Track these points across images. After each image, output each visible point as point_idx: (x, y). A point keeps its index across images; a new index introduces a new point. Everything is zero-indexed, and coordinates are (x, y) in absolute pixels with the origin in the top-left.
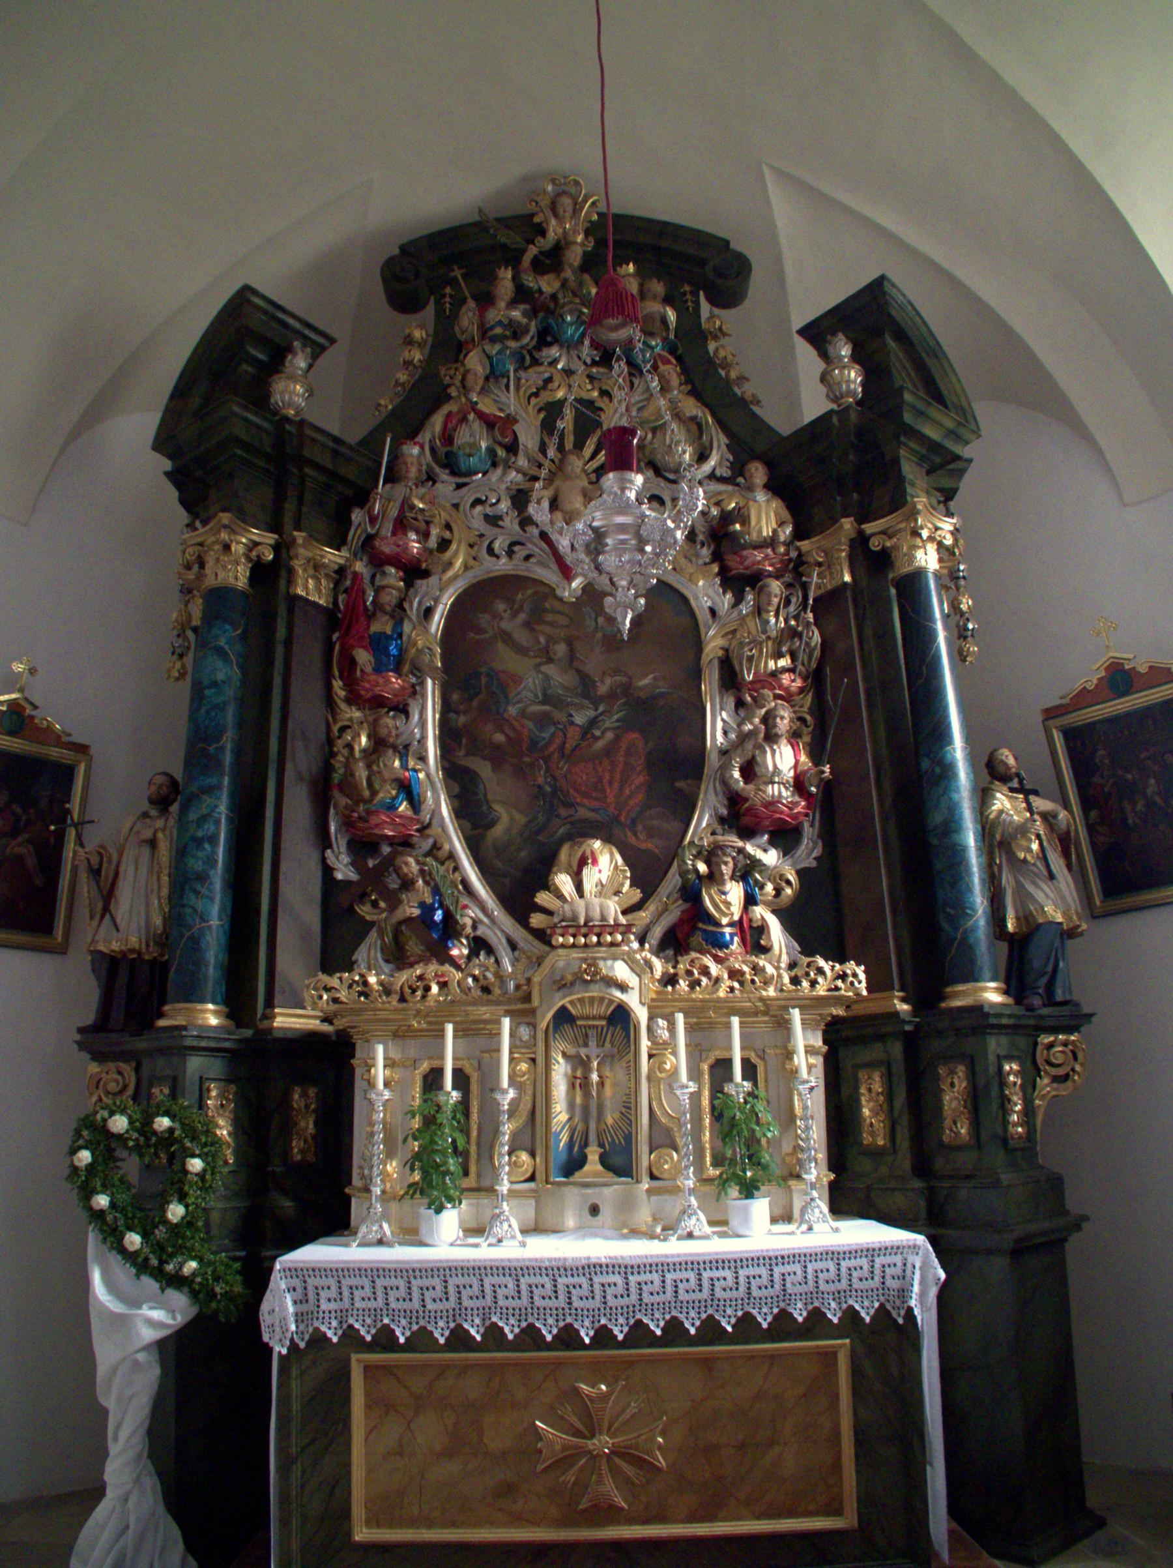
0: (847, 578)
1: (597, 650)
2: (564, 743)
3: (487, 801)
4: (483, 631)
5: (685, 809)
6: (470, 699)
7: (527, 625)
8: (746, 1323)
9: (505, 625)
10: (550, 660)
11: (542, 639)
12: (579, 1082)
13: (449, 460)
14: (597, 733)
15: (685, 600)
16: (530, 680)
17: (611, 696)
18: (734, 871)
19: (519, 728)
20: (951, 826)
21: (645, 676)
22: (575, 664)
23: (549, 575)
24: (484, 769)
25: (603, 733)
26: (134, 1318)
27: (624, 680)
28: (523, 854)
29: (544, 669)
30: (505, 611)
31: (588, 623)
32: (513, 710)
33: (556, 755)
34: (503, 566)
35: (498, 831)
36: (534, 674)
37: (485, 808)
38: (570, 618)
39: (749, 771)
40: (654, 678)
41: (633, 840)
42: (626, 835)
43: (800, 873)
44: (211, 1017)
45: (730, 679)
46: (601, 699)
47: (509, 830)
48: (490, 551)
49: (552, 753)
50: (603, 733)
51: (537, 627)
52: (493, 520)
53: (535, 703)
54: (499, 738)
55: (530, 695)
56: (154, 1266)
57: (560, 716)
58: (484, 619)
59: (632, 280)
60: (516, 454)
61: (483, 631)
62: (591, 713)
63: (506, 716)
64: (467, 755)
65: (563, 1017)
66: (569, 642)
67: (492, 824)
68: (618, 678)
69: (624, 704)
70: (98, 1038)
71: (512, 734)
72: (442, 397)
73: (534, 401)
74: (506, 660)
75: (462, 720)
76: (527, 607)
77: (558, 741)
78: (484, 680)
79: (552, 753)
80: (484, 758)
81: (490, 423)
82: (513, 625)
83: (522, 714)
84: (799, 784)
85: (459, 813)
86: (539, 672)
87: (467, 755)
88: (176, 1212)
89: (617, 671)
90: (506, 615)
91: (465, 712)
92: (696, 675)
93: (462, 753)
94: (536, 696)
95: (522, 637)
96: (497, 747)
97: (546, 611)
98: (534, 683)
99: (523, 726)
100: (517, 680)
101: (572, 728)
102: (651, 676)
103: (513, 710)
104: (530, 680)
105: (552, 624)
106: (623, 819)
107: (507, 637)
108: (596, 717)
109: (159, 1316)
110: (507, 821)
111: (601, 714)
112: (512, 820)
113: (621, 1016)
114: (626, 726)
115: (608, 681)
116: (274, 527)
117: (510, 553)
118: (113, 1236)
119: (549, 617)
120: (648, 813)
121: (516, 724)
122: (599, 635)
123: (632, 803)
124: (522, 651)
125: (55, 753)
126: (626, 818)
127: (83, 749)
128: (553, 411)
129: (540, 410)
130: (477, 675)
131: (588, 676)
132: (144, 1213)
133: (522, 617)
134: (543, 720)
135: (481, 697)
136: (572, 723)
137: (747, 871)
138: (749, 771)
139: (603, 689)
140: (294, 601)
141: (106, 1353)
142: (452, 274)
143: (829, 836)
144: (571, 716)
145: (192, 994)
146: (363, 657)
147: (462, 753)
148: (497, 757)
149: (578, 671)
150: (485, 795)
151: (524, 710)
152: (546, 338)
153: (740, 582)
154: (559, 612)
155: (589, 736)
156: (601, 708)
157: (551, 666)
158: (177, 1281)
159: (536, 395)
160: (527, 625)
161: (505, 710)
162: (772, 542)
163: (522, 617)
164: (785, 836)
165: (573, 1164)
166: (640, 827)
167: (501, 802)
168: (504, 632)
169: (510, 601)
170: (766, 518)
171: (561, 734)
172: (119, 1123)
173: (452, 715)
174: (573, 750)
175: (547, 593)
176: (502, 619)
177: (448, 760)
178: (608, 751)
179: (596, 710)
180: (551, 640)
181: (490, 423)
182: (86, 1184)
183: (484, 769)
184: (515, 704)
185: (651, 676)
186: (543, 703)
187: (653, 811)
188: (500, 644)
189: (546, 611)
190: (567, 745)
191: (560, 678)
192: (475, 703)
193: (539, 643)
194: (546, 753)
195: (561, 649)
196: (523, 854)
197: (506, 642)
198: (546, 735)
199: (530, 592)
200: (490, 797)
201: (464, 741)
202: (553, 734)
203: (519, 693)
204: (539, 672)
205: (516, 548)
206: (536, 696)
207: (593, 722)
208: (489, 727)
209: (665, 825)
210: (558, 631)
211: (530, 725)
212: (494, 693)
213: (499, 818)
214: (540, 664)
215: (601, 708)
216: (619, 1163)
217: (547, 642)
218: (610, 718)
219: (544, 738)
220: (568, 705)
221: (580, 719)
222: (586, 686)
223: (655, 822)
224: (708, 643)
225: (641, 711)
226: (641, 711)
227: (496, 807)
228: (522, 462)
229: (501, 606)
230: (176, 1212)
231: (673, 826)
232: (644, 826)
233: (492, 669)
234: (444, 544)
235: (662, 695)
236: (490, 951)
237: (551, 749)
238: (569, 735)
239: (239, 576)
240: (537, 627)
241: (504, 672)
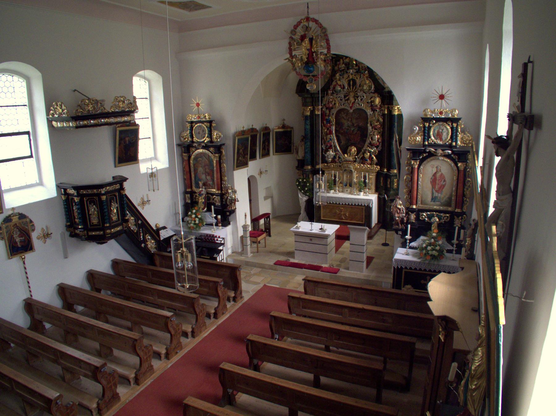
0: (386, 113)
5: (364, 142)
7: (346, 116)
8: (355, 205)
12: (347, 177)
13: (335, 91)
16: (346, 123)
20: (393, 150)
23: (349, 109)
24: (340, 135)
26: (303, 199)
34: (343, 107)
39: (372, 139)
43: (379, 151)
44: (309, 167)
45: (371, 125)
52: (341, 100)
56: (305, 193)
65: (345, 170)
70: (297, 168)
72: (333, 81)
81: (340, 86)
84: (378, 141)
88: (306, 189)
92: (367, 123)
95: (345, 117)
107: (343, 118)
109: (305, 198)
110: (343, 142)
113: (351, 171)
114: (358, 130)
116: (313, 105)
118: (301, 191)
124: (345, 119)
125: (289, 130)
127: (292, 128)
128: (349, 81)
132: (304, 190)
134: (347, 129)
137: (370, 152)
138: (372, 139)
140: (316, 115)
141: (300, 202)
143: (382, 147)
145: (308, 165)
146: (325, 122)
148: (342, 134)
152: (348, 69)
153: (373, 110)
158: (306, 195)
162: (377, 106)
164: (377, 147)
165: (346, 185)
170: (377, 101)
172: (300, 180)
175: (348, 111)
178: (356, 133)
181: (340, 86)
182: (298, 186)
183: (340, 135)
191: (350, 124)
216: (350, 186)
222: (353, 124)
225: (360, 128)
226: (360, 128)
228: (345, 90)
230: (306, 189)
234: (335, 104)
239: (308, 114)
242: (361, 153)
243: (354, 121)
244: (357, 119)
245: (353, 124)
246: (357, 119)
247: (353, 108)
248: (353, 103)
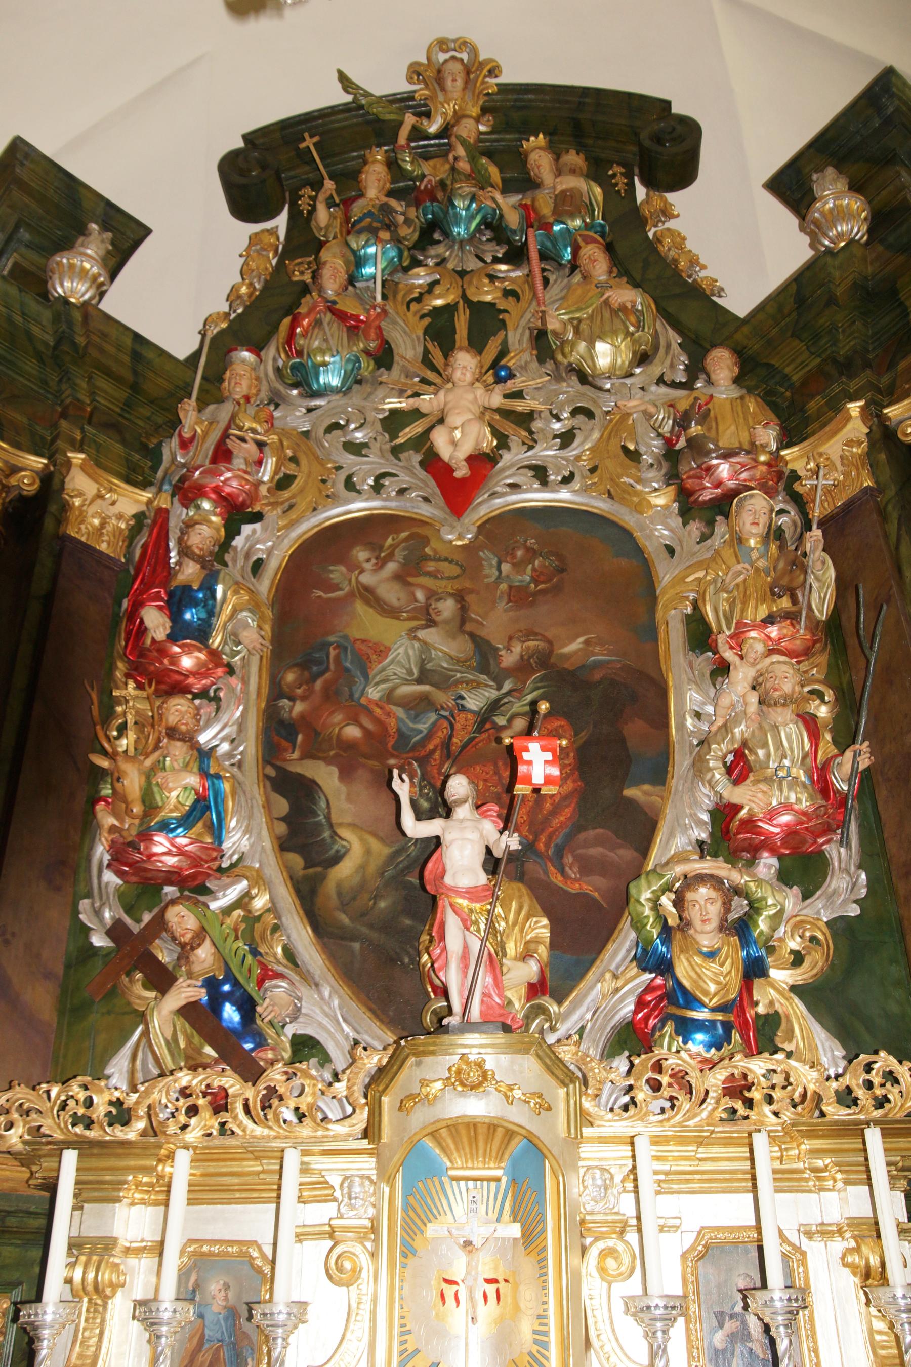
1: (502, 605)
2: (451, 737)
3: (331, 826)
4: (337, 588)
5: (641, 829)
6: (314, 678)
7: (400, 578)
9: (367, 579)
10: (431, 623)
11: (420, 595)
14: (501, 721)
15: (627, 534)
17: (523, 669)
18: (723, 920)
19: (383, 718)
21: (573, 639)
22: (468, 627)
24: (326, 776)
25: (510, 721)
27: (541, 645)
28: (382, 904)
29: (421, 634)
30: (368, 561)
31: (487, 571)
32: (374, 693)
33: (437, 755)
35: (345, 870)
36: (406, 641)
37: (326, 834)
38: (461, 566)
40: (587, 642)
41: (557, 879)
42: (546, 873)
46: (509, 672)
47: (362, 867)
48: (349, 484)
49: (433, 752)
50: (510, 721)
51: (411, 580)
53: (407, 682)
54: (353, 732)
55: (401, 672)
57: (443, 698)
58: (337, 572)
59: (542, 153)
60: (389, 367)
61: (337, 588)
62: (493, 694)
63: (363, 701)
64: (301, 759)
66: (460, 597)
67: (337, 859)
68: (531, 643)
69: (541, 679)
71: (369, 725)
73: (414, 306)
74: (366, 623)
75: (299, 707)
76: (399, 555)
77: (441, 734)
78: (333, 653)
79: (433, 752)
80: (328, 761)
82: (379, 578)
83: (389, 697)
85: (284, 846)
86: (416, 638)
87: (301, 759)
89: (529, 634)
90: (368, 566)
91: (303, 698)
93: (296, 755)
94: (410, 672)
95: (391, 594)
96: (349, 746)
97: (426, 558)
98: (406, 652)
99: (388, 714)
100: (382, 651)
101: (463, 716)
102: (581, 639)
103: (374, 693)
104: (401, 650)
105: (433, 575)
106: (541, 846)
107: (368, 595)
108: (498, 700)
111: (509, 693)
112: (368, 852)
115: (517, 649)
117: (377, 488)
119: (431, 566)
120: (582, 836)
121: (378, 711)
122: (504, 587)
123: (555, 822)
124: (391, 612)
126: (547, 845)
129: (423, 317)
130: (326, 646)
131: (488, 642)
133: (391, 567)
134: (419, 705)
135: (327, 676)
136: (463, 709)
139: (509, 659)
142: (303, 145)
144: (462, 698)
147: (296, 755)
148: (348, 759)
149: (472, 636)
150: (328, 817)
151: (392, 690)
154: (446, 560)
155: (488, 726)
156: (507, 686)
157: (432, 630)
159: (418, 300)
160: (400, 578)
161: (363, 693)
163: (391, 567)
166: (569, 859)
167: (353, 826)
168: (367, 589)
169: (375, 547)
171: (446, 724)
173: (285, 702)
174: (464, 747)
176: (362, 571)
177: (274, 766)
179: (499, 688)
180: (432, 595)
183: (326, 776)
184: (377, 684)
185: (581, 639)
186: (419, 681)
187: (591, 833)
188: (360, 607)
189: (426, 558)
190: (455, 740)
191: (444, 647)
192: (319, 684)
193: (416, 601)
194: (423, 753)
195: (447, 608)
196: (382, 904)
197: (367, 602)
198: (423, 727)
199: (404, 535)
200: (335, 818)
201: (300, 737)
202: (434, 724)
203: (383, 670)
204: (416, 638)
205: (386, 482)
206: (410, 672)
207: (494, 706)
208: (338, 718)
209: (611, 854)
210: (443, 583)
211: (400, 712)
212: (347, 670)
213: (347, 851)
214: (417, 629)
215: (507, 686)
217: (428, 599)
218: (519, 699)
219: (421, 732)
220: (459, 682)
221: (474, 702)
222: (484, 656)
223: (596, 851)
224: (664, 592)
227: (344, 833)
229: (361, 555)
231: (626, 854)
232: (578, 859)
233: (346, 637)
235: (598, 665)
236: (325, 1059)
237: (431, 747)
238: (458, 726)
240: (411, 580)
241: (364, 641)
242: (623, 945)
243: (496, 622)
244: (519, 597)
245: (484, 656)
246: (519, 597)
247: (488, 505)
248: (482, 462)
